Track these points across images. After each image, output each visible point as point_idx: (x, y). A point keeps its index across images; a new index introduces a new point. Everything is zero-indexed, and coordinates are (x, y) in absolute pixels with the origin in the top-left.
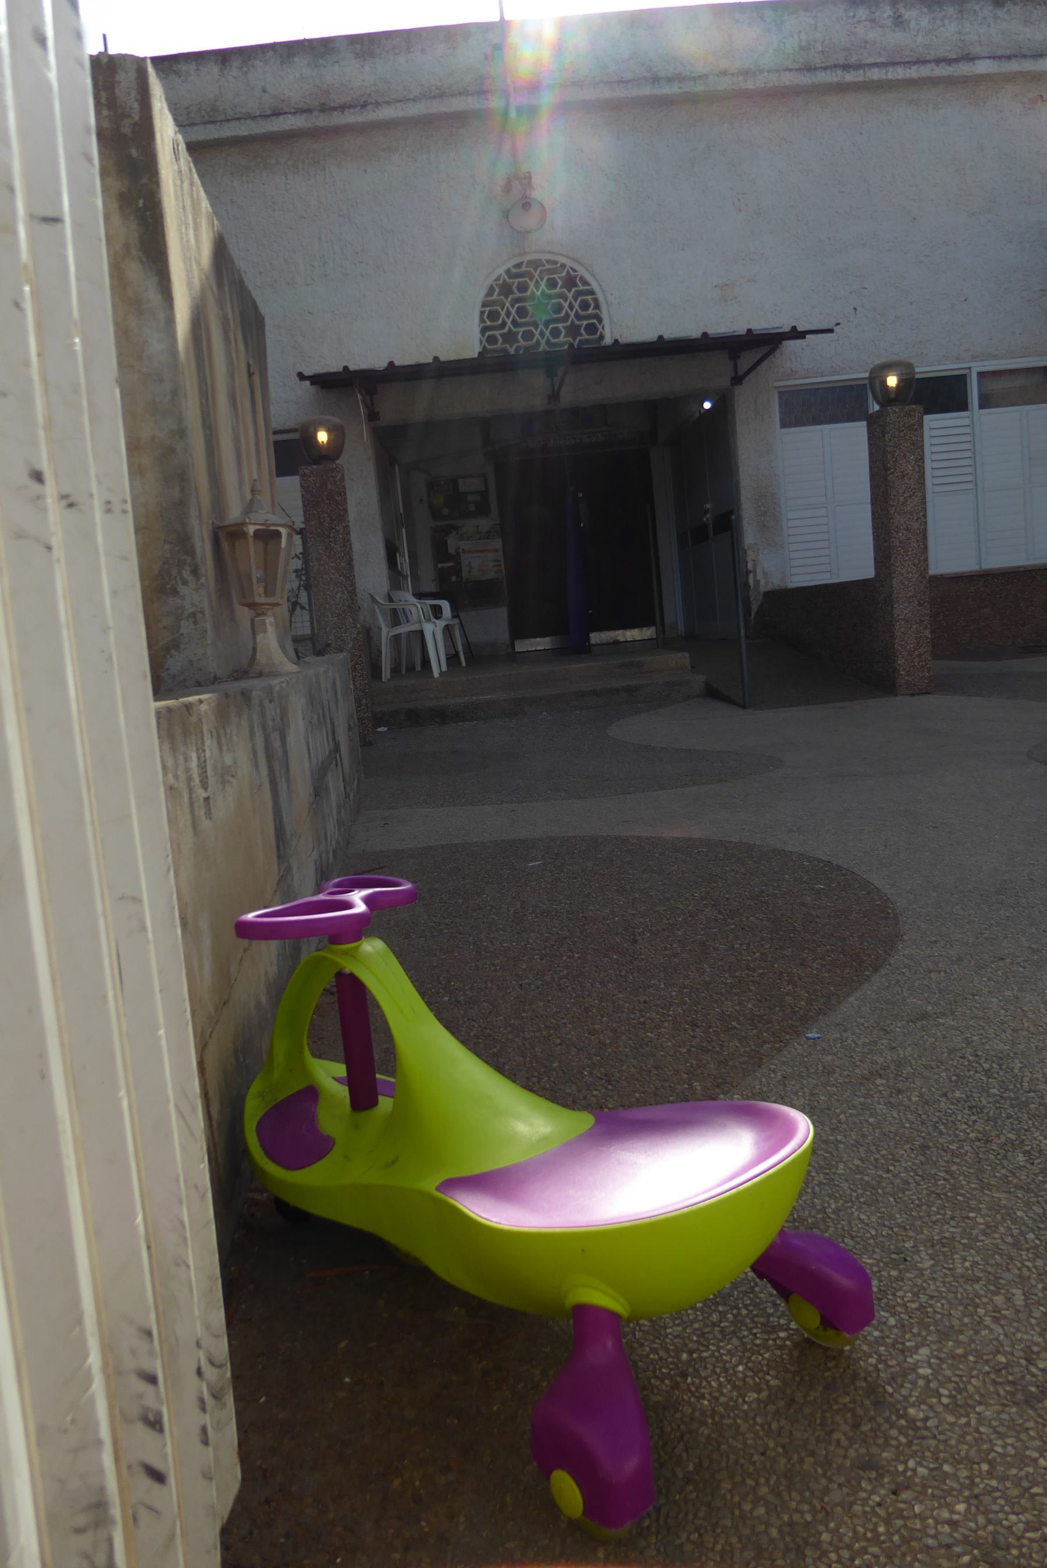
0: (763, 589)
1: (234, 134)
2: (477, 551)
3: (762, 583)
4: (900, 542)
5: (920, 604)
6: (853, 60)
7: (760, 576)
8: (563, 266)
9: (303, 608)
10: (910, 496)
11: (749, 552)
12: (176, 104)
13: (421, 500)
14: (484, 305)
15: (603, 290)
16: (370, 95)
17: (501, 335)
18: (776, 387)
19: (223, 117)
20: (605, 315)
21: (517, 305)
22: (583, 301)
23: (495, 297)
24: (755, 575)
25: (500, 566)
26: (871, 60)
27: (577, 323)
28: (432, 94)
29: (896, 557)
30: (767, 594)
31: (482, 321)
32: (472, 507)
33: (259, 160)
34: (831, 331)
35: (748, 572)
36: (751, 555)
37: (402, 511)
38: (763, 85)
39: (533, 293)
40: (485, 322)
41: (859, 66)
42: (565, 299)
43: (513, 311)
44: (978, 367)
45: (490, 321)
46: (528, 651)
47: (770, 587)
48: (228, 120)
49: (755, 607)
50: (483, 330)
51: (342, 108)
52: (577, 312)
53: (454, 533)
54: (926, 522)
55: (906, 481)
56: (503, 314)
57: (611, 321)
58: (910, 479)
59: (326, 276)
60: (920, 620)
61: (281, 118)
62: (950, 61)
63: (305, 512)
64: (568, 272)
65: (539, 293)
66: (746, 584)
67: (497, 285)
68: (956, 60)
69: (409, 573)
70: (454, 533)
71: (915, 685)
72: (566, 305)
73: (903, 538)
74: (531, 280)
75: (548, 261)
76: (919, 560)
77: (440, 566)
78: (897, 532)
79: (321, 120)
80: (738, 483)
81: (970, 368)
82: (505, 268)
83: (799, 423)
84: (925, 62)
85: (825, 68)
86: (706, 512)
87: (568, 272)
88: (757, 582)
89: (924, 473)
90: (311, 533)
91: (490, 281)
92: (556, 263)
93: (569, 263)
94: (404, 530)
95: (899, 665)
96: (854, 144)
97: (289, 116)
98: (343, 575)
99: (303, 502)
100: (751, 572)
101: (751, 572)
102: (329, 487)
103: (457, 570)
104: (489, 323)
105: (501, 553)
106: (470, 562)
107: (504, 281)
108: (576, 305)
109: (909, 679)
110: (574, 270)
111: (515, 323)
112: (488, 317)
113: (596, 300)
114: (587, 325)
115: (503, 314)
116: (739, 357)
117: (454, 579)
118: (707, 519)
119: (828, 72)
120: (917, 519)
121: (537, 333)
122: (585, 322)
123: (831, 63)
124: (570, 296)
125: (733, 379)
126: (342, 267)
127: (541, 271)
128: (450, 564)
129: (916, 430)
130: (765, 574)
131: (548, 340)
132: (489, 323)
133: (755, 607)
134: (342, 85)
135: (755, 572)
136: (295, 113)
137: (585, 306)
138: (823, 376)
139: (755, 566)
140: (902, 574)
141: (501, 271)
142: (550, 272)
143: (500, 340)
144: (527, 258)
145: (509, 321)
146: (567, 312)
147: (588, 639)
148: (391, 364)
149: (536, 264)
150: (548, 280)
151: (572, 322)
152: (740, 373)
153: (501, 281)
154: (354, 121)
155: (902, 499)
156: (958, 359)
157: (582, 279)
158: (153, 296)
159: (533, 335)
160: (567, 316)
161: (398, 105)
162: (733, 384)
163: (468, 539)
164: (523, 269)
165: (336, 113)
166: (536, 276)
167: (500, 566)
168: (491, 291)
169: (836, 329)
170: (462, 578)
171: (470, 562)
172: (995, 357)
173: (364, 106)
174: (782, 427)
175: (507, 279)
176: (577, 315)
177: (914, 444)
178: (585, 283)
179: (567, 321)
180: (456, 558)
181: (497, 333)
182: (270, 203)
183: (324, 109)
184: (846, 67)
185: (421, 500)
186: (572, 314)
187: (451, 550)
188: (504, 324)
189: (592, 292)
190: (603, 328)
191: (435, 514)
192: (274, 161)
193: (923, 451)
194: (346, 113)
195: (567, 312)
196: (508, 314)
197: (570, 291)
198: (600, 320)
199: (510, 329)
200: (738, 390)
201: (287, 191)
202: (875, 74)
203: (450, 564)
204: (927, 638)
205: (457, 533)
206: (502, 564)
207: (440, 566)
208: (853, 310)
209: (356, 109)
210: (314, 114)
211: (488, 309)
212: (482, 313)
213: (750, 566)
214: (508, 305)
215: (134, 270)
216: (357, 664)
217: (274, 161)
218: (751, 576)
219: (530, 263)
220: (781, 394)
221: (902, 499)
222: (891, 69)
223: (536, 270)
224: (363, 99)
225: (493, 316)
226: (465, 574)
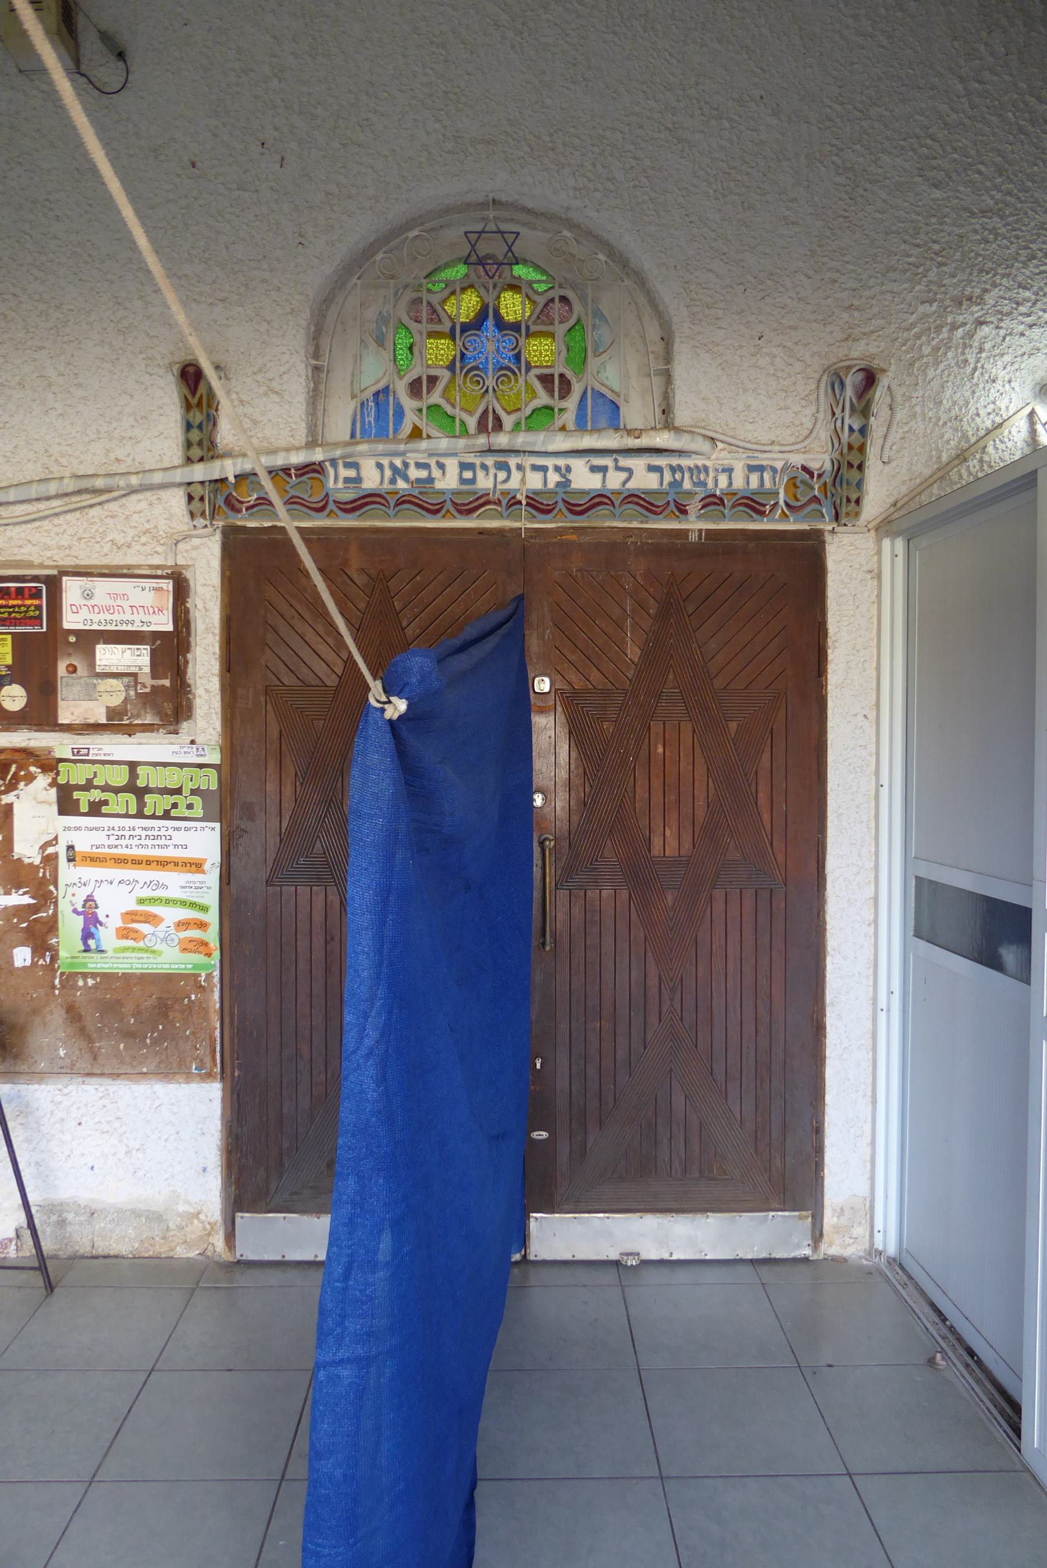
2: (121, 861)
9: (175, 806)
25: (202, 925)
53: (42, 781)
105: (212, 878)
106: (90, 899)
117: (22, 956)
128: (20, 899)
147: (523, 1240)
163: (95, 809)
167: (202, 925)
170: (54, 958)
171: (90, 899)
203: (20, 899)
205: (54, 783)
206: (213, 917)
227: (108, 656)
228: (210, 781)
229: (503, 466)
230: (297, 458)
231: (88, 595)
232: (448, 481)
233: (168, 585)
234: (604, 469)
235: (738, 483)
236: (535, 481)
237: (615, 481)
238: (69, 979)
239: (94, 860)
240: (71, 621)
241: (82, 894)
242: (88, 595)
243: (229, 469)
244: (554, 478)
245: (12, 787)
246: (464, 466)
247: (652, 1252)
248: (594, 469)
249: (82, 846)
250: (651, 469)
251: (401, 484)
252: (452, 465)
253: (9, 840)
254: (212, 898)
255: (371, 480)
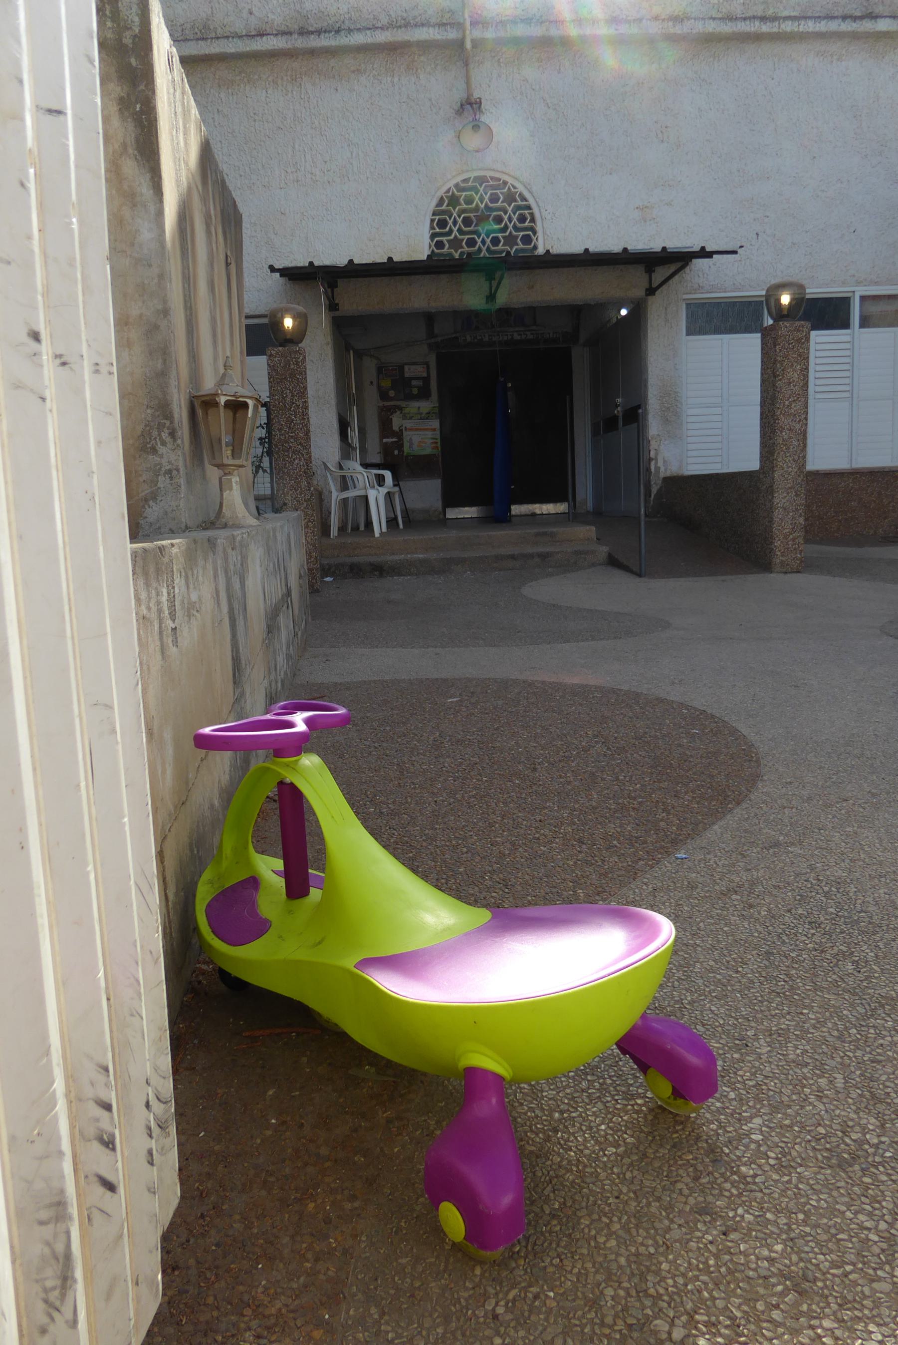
0: (662, 475)
1: (222, 50)
2: (417, 430)
3: (662, 469)
4: (783, 440)
5: (797, 495)
6: (770, 12)
7: (660, 464)
8: (505, 183)
9: (264, 471)
10: (794, 401)
11: (653, 443)
12: (172, 21)
13: (372, 383)
14: (434, 214)
15: (539, 206)
16: (343, 22)
17: (448, 241)
18: (684, 300)
19: (213, 35)
20: (539, 228)
21: (463, 216)
22: (520, 215)
23: (444, 207)
24: (656, 463)
26: (786, 13)
27: (514, 233)
28: (398, 24)
29: (779, 453)
30: (665, 479)
31: (432, 228)
32: (415, 391)
33: (243, 75)
34: (735, 252)
35: (650, 460)
36: (653, 445)
37: (354, 392)
38: (689, 31)
39: (477, 205)
40: (434, 229)
41: (775, 19)
42: (506, 213)
43: (460, 220)
44: (861, 291)
45: (439, 229)
46: (457, 518)
47: (668, 474)
48: (218, 38)
49: (654, 490)
50: (433, 236)
51: (319, 32)
52: (515, 223)
53: (398, 412)
54: (806, 425)
55: (792, 387)
56: (450, 222)
57: (544, 233)
58: (794, 386)
59: (298, 181)
60: (796, 509)
61: (265, 38)
62: (855, 19)
63: (270, 388)
64: (509, 188)
65: (483, 206)
66: (648, 470)
67: (446, 197)
68: (861, 18)
69: (358, 445)
70: (398, 412)
71: (788, 565)
72: (506, 218)
73: (786, 437)
74: (477, 194)
75: (492, 178)
76: (799, 457)
77: (385, 440)
78: (781, 432)
79: (300, 43)
80: (646, 381)
81: (854, 292)
82: (454, 182)
83: (702, 332)
84: (834, 18)
85: (745, 19)
86: (617, 406)
87: (509, 188)
88: (658, 469)
89: (807, 381)
90: (274, 406)
91: (441, 193)
92: (500, 180)
93: (510, 181)
94: (355, 408)
95: (775, 546)
96: (766, 89)
97: (272, 37)
98: (301, 444)
99: (269, 379)
100: (653, 459)
101: (653, 459)
102: (292, 367)
103: (399, 445)
104: (438, 230)
105: (438, 432)
107: (453, 193)
108: (515, 219)
109: (784, 559)
110: (515, 187)
111: (460, 231)
112: (437, 225)
113: (532, 215)
114: (523, 236)
115: (450, 222)
116: (654, 271)
117: (396, 452)
118: (618, 411)
119: (748, 22)
120: (799, 421)
121: (479, 241)
122: (522, 233)
123: (750, 14)
124: (510, 209)
125: (647, 290)
126: (312, 174)
127: (486, 186)
128: (394, 440)
129: (803, 343)
130: (665, 461)
131: (488, 248)
132: (438, 230)
133: (654, 490)
134: (320, 11)
135: (656, 459)
136: (276, 35)
137: (522, 219)
138: (725, 292)
139: (657, 454)
140: (783, 468)
141: (451, 184)
142: (493, 187)
143: (447, 246)
144: (472, 175)
145: (455, 229)
146: (506, 224)
147: (510, 510)
148: (351, 261)
149: (481, 180)
150: (491, 194)
151: (511, 232)
152: (654, 285)
153: (450, 193)
154: (329, 44)
155: (787, 403)
156: (844, 283)
157: (521, 195)
158: (146, 191)
159: (476, 243)
160: (506, 227)
161: (368, 32)
162: (647, 295)
163: (411, 418)
164: (470, 184)
165: (313, 36)
166: (481, 190)
167: (437, 443)
168: (441, 202)
169: (739, 251)
170: (403, 452)
172: (876, 283)
173: (338, 31)
174: (688, 334)
175: (456, 192)
176: (515, 228)
177: (800, 356)
178: (524, 199)
179: (505, 232)
180: (399, 435)
181: (444, 239)
182: (252, 115)
183: (303, 32)
184: (763, 19)
185: (372, 383)
186: (511, 226)
187: (395, 428)
188: (451, 231)
189: (529, 207)
190: (537, 239)
191: (384, 396)
192: (256, 77)
193: (808, 362)
194: (322, 36)
195: (506, 224)
196: (455, 223)
197: (509, 206)
198: (535, 233)
199: (456, 236)
200: (651, 299)
201: (267, 104)
202: (788, 27)
203: (394, 440)
204: (801, 524)
206: (439, 441)
207: (385, 440)
208: (755, 236)
209: (331, 35)
210: (293, 36)
211: (437, 217)
212: (432, 221)
213: (652, 454)
214: (455, 214)
215: (130, 167)
216: (310, 521)
217: (256, 77)
218: (653, 464)
219: (476, 179)
220: (687, 305)
221: (787, 403)
222: (803, 22)
223: (481, 185)
224: (338, 25)
225: (442, 224)
226: (406, 449)
227: (414, 383)
228: (437, 410)
229: (498, 335)
230: (454, 336)
231: (409, 369)
232: (486, 339)
233: (425, 366)
234: (521, 335)
235: (551, 336)
236: (505, 338)
237: (524, 337)
238: (407, 457)
239: (411, 430)
240: (407, 375)
241: (409, 438)
242: (409, 369)
243: (439, 339)
244: (510, 337)
245: (392, 414)
246: (489, 336)
247: (538, 512)
248: (519, 335)
249: (408, 426)
250: (532, 334)
251: (476, 340)
252: (487, 335)
253: (392, 427)
254: (438, 436)
255: (469, 339)
